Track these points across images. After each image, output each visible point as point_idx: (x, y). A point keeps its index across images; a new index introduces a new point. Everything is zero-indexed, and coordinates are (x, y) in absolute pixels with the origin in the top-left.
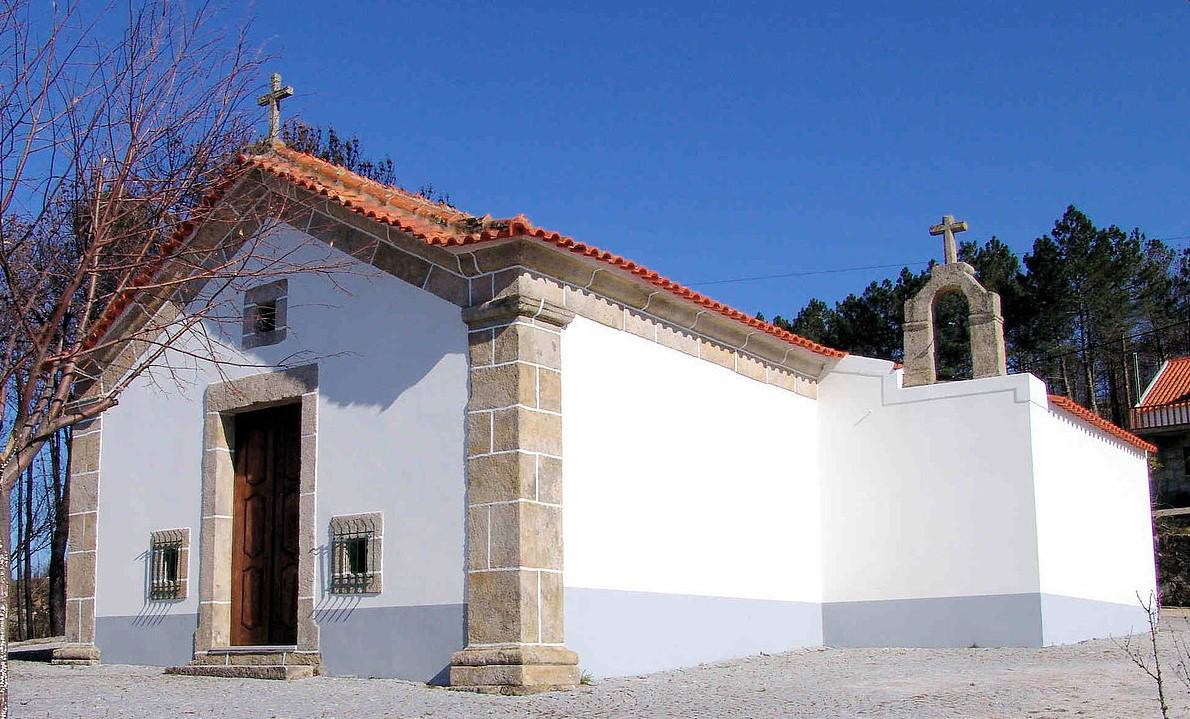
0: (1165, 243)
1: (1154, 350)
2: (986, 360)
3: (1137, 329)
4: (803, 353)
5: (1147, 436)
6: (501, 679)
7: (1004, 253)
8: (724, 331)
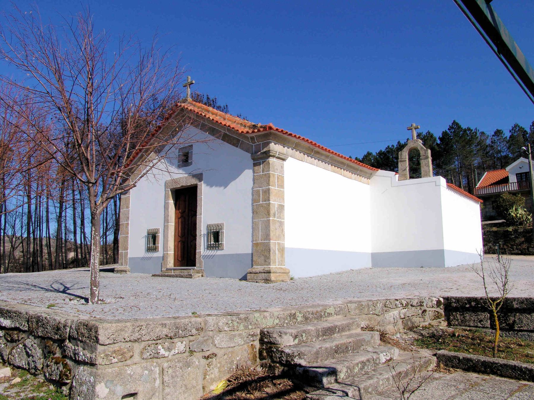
0: (485, 133)
1: (482, 168)
2: (426, 172)
3: (476, 161)
4: (365, 169)
5: (480, 197)
6: (264, 278)
7: (432, 136)
8: (338, 162)
